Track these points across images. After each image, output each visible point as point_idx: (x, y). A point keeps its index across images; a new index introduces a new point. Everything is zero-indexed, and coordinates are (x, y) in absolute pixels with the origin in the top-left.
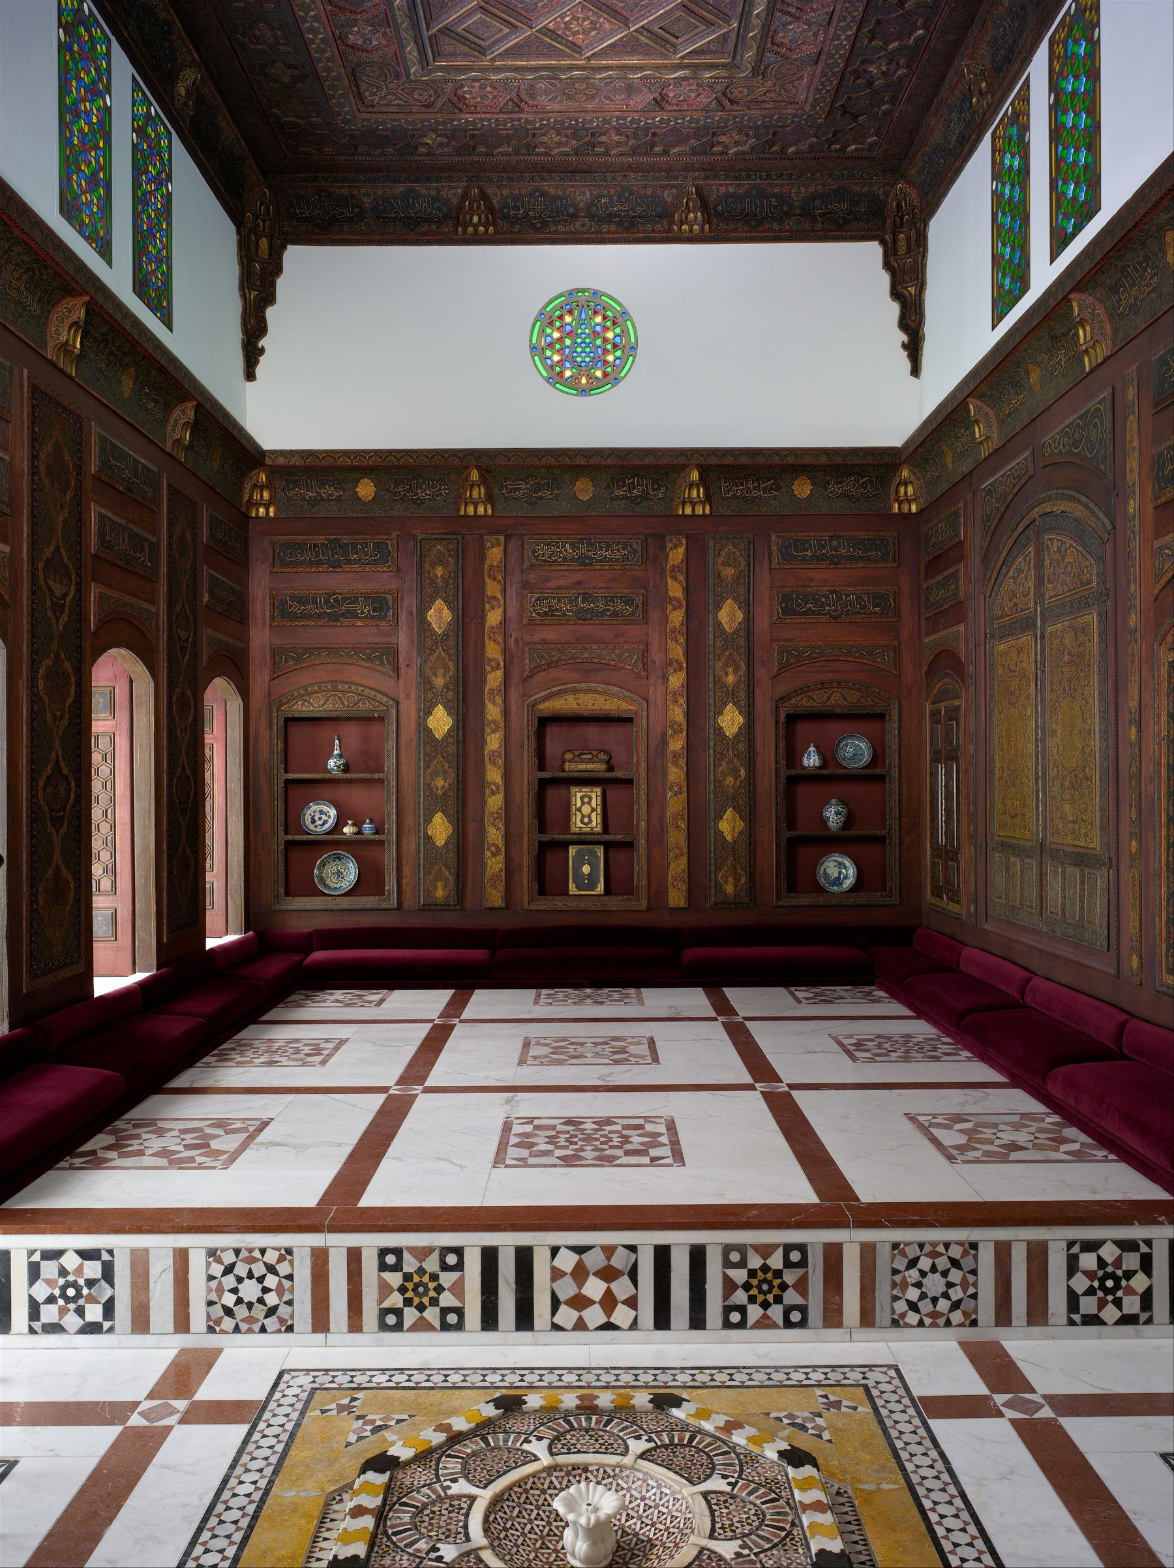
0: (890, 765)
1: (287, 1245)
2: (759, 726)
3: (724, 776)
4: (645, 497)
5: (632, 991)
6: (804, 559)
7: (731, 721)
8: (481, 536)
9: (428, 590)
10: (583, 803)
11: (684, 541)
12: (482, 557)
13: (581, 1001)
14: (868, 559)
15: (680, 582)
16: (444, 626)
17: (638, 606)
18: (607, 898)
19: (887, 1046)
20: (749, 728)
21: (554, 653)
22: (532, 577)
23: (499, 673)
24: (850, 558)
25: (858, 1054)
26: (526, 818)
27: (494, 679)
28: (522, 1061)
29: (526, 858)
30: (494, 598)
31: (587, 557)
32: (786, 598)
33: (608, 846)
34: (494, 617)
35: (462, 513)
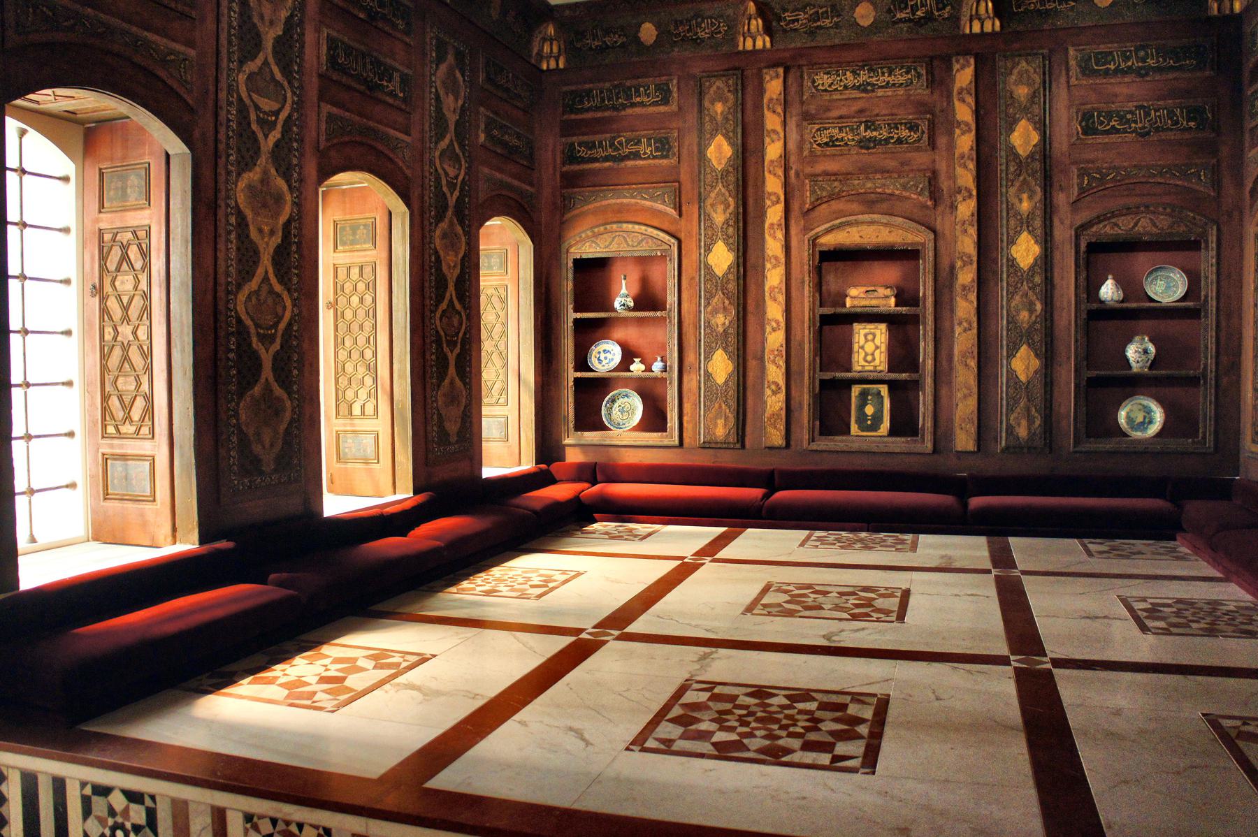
0: (1206, 296)
1: (327, 824)
2: (1057, 256)
3: (1018, 311)
4: (929, 18)
5: (908, 537)
6: (1107, 72)
7: (1025, 251)
8: (760, 70)
9: (708, 127)
10: (867, 340)
11: (972, 61)
12: (761, 91)
13: (849, 545)
14: (1181, 68)
15: (969, 105)
16: (724, 162)
17: (923, 132)
18: (890, 439)
19: (1187, 614)
20: (1046, 261)
21: (836, 184)
22: (812, 109)
23: (780, 207)
24: (1159, 70)
25: (1150, 623)
26: (807, 356)
27: (774, 214)
28: (906, 594)
29: (806, 397)
30: (774, 131)
31: (868, 84)
32: (1087, 117)
33: (893, 386)
34: (773, 151)
35: (741, 48)
